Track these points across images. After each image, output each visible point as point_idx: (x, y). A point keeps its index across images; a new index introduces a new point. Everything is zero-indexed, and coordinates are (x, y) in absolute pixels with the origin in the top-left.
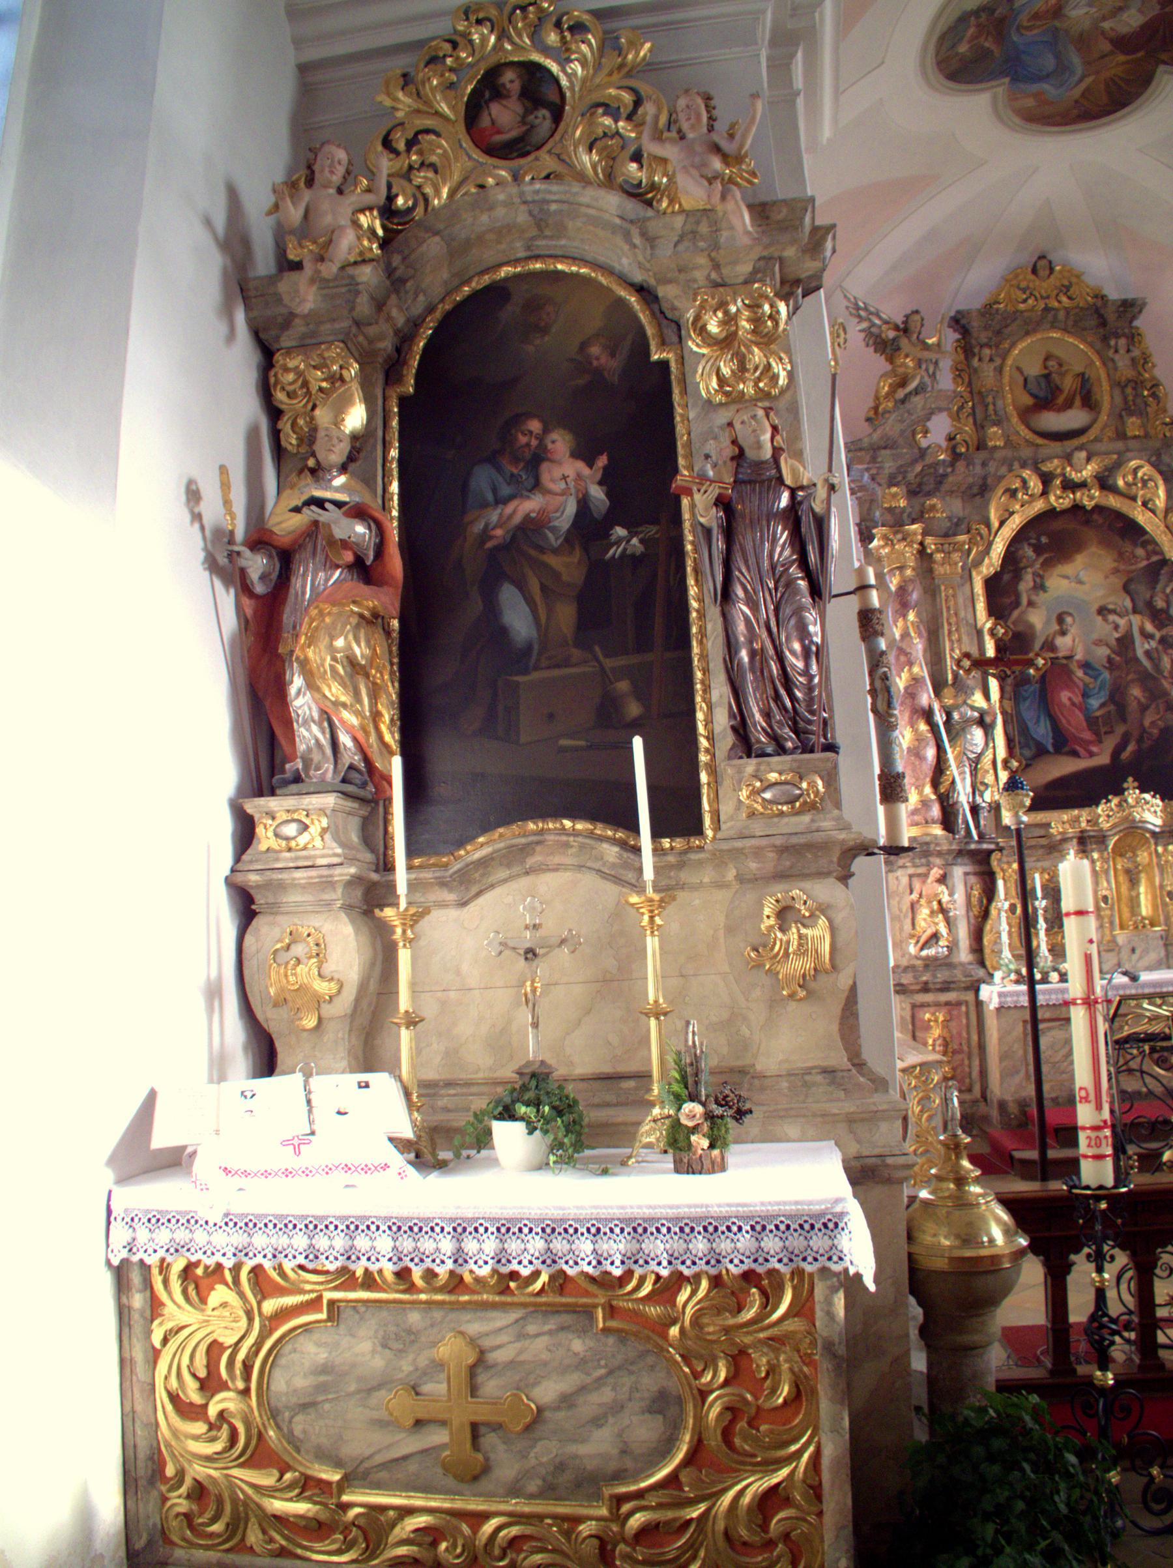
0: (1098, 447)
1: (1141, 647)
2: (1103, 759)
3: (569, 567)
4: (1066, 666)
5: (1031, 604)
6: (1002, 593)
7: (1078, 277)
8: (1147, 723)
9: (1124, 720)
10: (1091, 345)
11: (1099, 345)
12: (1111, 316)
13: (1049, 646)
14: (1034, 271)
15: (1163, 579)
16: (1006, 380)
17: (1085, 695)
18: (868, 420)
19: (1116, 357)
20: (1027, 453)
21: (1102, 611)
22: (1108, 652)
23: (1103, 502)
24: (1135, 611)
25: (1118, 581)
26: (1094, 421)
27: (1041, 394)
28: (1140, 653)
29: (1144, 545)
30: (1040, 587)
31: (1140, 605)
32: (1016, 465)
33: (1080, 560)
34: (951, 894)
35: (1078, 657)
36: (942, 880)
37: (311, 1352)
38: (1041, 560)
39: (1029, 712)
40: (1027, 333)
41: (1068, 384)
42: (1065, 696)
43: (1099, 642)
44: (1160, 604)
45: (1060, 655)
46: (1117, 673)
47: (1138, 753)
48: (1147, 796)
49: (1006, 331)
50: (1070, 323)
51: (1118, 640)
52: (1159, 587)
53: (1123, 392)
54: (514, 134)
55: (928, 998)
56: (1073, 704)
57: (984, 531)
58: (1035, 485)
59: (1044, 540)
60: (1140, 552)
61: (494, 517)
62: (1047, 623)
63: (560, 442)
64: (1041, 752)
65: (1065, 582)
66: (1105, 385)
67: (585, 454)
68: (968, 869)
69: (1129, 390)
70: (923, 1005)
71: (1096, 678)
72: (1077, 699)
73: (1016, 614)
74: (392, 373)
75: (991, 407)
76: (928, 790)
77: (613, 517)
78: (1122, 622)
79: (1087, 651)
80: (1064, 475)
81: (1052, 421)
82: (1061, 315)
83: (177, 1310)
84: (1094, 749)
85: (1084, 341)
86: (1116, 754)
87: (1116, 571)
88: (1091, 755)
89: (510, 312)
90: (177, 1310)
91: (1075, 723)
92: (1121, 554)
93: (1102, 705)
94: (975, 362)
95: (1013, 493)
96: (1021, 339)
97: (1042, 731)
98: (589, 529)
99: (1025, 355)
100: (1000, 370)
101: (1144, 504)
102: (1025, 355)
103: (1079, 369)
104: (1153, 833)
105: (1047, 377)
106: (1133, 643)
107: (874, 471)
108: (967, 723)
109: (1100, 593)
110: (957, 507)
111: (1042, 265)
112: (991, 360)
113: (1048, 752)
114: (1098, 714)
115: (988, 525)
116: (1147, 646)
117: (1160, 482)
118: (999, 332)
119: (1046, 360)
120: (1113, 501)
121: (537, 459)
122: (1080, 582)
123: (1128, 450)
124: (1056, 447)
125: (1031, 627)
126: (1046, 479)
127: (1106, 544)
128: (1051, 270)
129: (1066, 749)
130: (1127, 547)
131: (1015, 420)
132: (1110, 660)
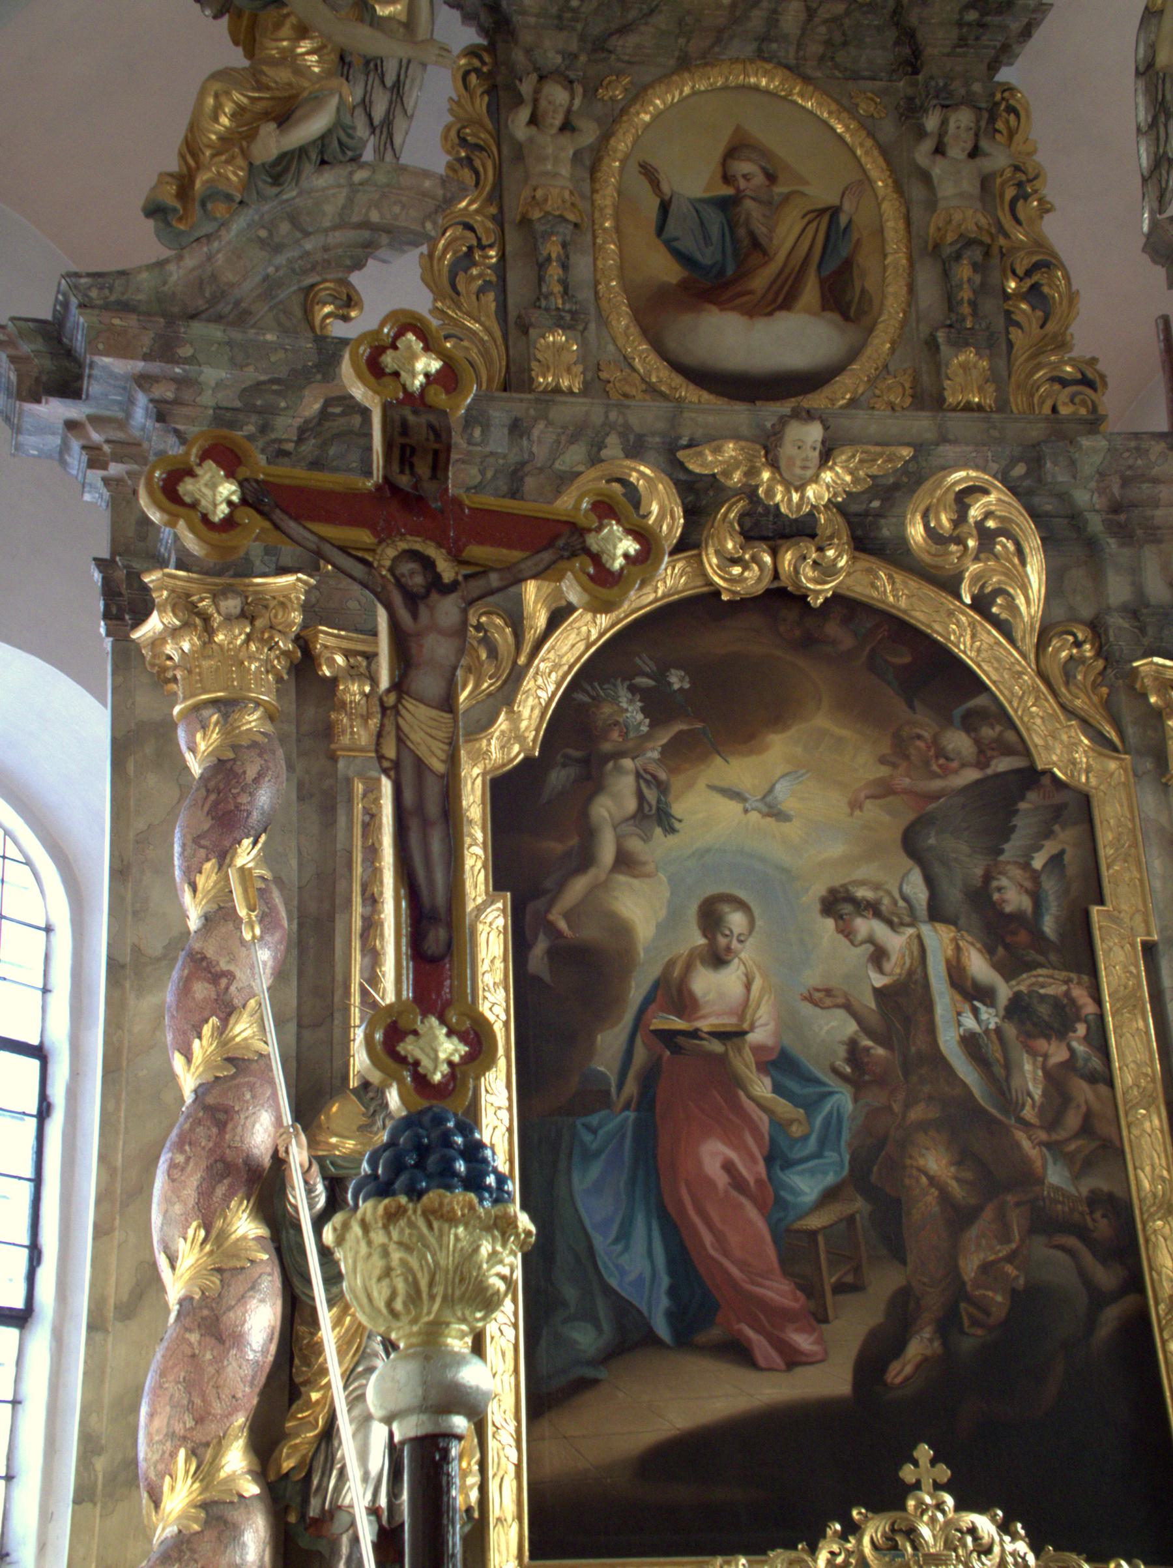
0: (860, 422)
1: (952, 1024)
2: (830, 1380)
4: (722, 1059)
5: (625, 862)
8: (970, 1266)
9: (897, 1252)
10: (868, 126)
11: (888, 129)
13: (673, 993)
15: (1025, 824)
16: (607, 197)
17: (777, 1157)
18: (155, 211)
19: (938, 169)
20: (647, 416)
21: (837, 903)
22: (852, 1027)
23: (860, 589)
24: (936, 913)
25: (888, 822)
26: (853, 355)
27: (707, 256)
28: (948, 1041)
29: (970, 723)
30: (656, 815)
31: (954, 895)
32: (613, 447)
35: (759, 1036)
38: (664, 737)
40: (684, 64)
41: (788, 235)
42: (713, 1155)
43: (824, 997)
44: (1013, 897)
45: (704, 1025)
46: (876, 1097)
48: (985, 1525)
49: (627, 44)
50: (814, 49)
51: (878, 993)
52: (1012, 848)
53: (946, 274)
56: (738, 1183)
57: (503, 636)
58: (664, 511)
59: (677, 680)
60: (959, 742)
62: (670, 924)
64: (631, 1339)
65: (735, 807)
66: (897, 254)
69: (964, 271)
71: (810, 1106)
72: (753, 1170)
73: (578, 887)
75: (554, 271)
76: (235, 1460)
78: (896, 942)
79: (787, 1021)
80: (750, 493)
81: (733, 338)
84: (803, 1341)
85: (848, 109)
86: (871, 1365)
87: (883, 790)
88: (793, 1360)
91: (740, 1244)
92: (900, 749)
93: (830, 1196)
94: (519, 124)
96: (664, 78)
97: (635, 1266)
100: (591, 163)
101: (981, 605)
103: (823, 193)
105: (726, 205)
106: (928, 1005)
107: (167, 392)
109: (836, 849)
112: (567, 127)
113: (651, 1340)
114: (814, 1222)
115: (516, 621)
116: (969, 1022)
117: (1033, 543)
119: (731, 153)
120: (890, 590)
122: (777, 814)
123: (944, 439)
124: (740, 414)
125: (622, 930)
126: (699, 498)
127: (859, 708)
129: (715, 1333)
130: (924, 724)
131: (622, 321)
132: (854, 1051)
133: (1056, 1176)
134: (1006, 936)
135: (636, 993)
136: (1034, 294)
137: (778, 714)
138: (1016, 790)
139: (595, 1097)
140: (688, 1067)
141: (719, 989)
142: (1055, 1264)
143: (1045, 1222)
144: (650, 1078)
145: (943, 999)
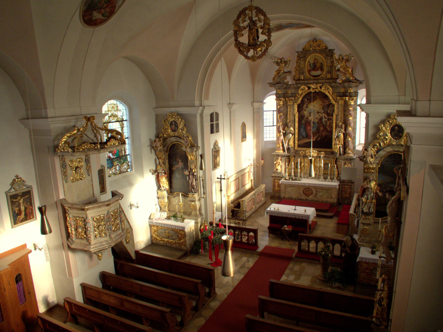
1: (324, 120)
5: (305, 110)
6: (300, 108)
9: (319, 133)
10: (324, 57)
12: (327, 52)
13: (307, 118)
14: (313, 41)
15: (330, 107)
21: (318, 112)
25: (321, 107)
30: (307, 107)
39: (302, 130)
41: (318, 65)
42: (309, 128)
43: (316, 118)
44: (329, 112)
55: (276, 178)
60: (327, 101)
63: (180, 161)
64: (303, 137)
67: (182, 162)
73: (302, 112)
78: (321, 115)
79: (314, 120)
82: (318, 51)
83: (153, 228)
85: (323, 56)
86: (316, 139)
87: (322, 105)
90: (153, 228)
97: (304, 134)
99: (310, 59)
102: (310, 59)
103: (321, 62)
105: (314, 63)
109: (318, 109)
110: (293, 91)
121: (178, 162)
125: (304, 114)
130: (325, 100)
131: (307, 73)
133: (329, 129)
134: (328, 114)
138: (330, 105)
141: (309, 118)
142: (328, 134)
143: (328, 132)
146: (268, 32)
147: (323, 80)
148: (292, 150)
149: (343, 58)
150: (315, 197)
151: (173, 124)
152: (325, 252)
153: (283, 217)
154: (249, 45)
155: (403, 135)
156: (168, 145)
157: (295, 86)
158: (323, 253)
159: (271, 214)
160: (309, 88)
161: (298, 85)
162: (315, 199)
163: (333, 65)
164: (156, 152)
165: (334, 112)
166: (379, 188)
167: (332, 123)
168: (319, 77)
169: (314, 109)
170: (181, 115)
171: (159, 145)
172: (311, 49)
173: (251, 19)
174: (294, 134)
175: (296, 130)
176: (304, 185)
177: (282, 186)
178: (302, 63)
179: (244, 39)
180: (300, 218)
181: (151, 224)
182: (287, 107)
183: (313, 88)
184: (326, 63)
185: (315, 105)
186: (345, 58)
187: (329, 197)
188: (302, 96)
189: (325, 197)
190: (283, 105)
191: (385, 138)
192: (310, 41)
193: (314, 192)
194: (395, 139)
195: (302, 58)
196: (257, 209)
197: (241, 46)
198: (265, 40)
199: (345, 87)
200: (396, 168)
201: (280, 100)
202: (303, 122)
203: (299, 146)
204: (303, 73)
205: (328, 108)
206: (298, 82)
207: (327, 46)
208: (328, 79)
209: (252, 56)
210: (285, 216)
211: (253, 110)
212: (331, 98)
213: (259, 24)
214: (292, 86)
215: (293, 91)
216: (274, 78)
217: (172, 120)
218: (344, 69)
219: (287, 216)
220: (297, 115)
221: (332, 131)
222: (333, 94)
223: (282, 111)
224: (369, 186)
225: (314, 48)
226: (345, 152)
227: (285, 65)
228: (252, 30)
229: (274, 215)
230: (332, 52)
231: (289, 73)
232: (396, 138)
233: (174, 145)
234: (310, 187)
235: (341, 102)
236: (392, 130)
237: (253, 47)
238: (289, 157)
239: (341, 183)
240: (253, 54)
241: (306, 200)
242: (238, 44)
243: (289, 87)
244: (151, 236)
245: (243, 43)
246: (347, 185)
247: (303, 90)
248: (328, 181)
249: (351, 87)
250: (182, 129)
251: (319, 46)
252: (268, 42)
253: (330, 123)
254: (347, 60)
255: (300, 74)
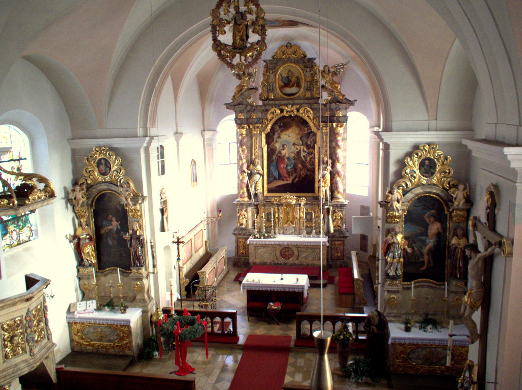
1: (303, 154)
2: (290, 182)
3: (116, 236)
5: (276, 141)
6: (269, 139)
7: (299, 48)
8: (301, 173)
10: (301, 68)
11: (303, 68)
12: (306, 62)
13: (280, 153)
15: (311, 136)
17: (287, 166)
21: (294, 144)
24: (302, 145)
25: (299, 137)
27: (286, 82)
28: (302, 156)
29: (307, 127)
30: (279, 137)
31: (304, 143)
33: (290, 130)
34: (247, 214)
36: (246, 211)
37: (87, 330)
39: (273, 169)
40: (284, 64)
41: (294, 79)
42: (282, 166)
43: (292, 152)
44: (309, 143)
47: (298, 181)
54: (104, 172)
55: (241, 236)
59: (282, 124)
60: (306, 129)
61: (106, 228)
62: (280, 147)
63: (114, 219)
64: (275, 179)
65: (285, 136)
67: (117, 221)
68: (253, 207)
70: (240, 238)
72: (285, 167)
73: (272, 144)
74: (91, 205)
77: (121, 230)
79: (289, 155)
81: (288, 90)
82: (293, 60)
85: (300, 67)
87: (299, 134)
88: (287, 180)
89: (106, 198)
91: (284, 172)
92: (301, 129)
95: (273, 113)
97: (276, 174)
98: (118, 231)
99: (282, 71)
102: (282, 71)
103: (297, 75)
104: (295, 205)
105: (288, 77)
108: (255, 174)
109: (294, 139)
110: (260, 115)
111: (289, 45)
113: (276, 179)
115: (267, 120)
118: (276, 64)
121: (111, 221)
122: (289, 136)
125: (276, 147)
127: (298, 126)
128: (291, 46)
130: (303, 127)
132: (294, 157)
133: (309, 166)
134: (308, 146)
135: (277, 153)
136: (316, 84)
137: (290, 127)
139: (273, 161)
140: (281, 159)
141: (283, 152)
142: (308, 173)
143: (308, 170)
144: (277, 160)
145: (302, 152)
146: (261, 31)
147: (300, 99)
148: (260, 196)
149: (329, 71)
150: (297, 259)
151: (101, 164)
152: (344, 335)
153: (266, 291)
154: (234, 46)
155: (435, 171)
156: (93, 196)
157: (263, 108)
158: (342, 337)
159: (249, 289)
160: (282, 111)
161: (267, 107)
162: (297, 262)
163: (313, 80)
164: (73, 208)
165: (316, 143)
166: (407, 242)
167: (314, 158)
168: (296, 96)
169: (289, 141)
170: (116, 151)
171: (80, 196)
172: (283, 57)
173: (237, 8)
174: (262, 175)
175: (266, 170)
176: (281, 243)
177: (250, 247)
178: (272, 76)
179: (227, 38)
180: (291, 290)
181: (71, 321)
182: (252, 138)
183: (287, 111)
184: (304, 77)
185: (290, 135)
186: (332, 70)
187: (317, 258)
188: (272, 122)
189: (310, 259)
190: (247, 134)
191: (412, 176)
192: (282, 46)
193: (296, 253)
194: (426, 177)
195: (272, 69)
196: (220, 283)
197: (223, 49)
198: (258, 41)
199: (331, 109)
200: (428, 214)
201: (243, 128)
202: (274, 158)
203: (270, 191)
204: (273, 91)
205: (308, 138)
206: (266, 102)
207: (306, 53)
208: (308, 99)
209: (238, 64)
210: (269, 289)
211: (204, 141)
212: (311, 124)
213: (251, 18)
214: (259, 108)
215: (260, 115)
216: (234, 96)
217: (100, 157)
218: (331, 84)
219: (272, 289)
220: (265, 149)
221: (314, 169)
222: (314, 119)
223: (245, 143)
224: (395, 241)
225: (288, 56)
226: (333, 197)
227: (249, 79)
228: (240, 25)
229: (253, 289)
230: (312, 62)
231: (254, 90)
232: (427, 175)
233: (104, 195)
234: (290, 247)
235: (326, 130)
236: (422, 165)
237: (240, 51)
238: (256, 207)
239: (330, 239)
240: (239, 60)
241: (285, 264)
242: (218, 46)
243: (255, 110)
244: (72, 340)
245: (226, 45)
246: (338, 241)
247: (273, 113)
248: (313, 237)
249: (339, 109)
250: (117, 172)
251: (295, 53)
252: (262, 43)
253: (310, 159)
254: (335, 74)
255: (269, 91)
